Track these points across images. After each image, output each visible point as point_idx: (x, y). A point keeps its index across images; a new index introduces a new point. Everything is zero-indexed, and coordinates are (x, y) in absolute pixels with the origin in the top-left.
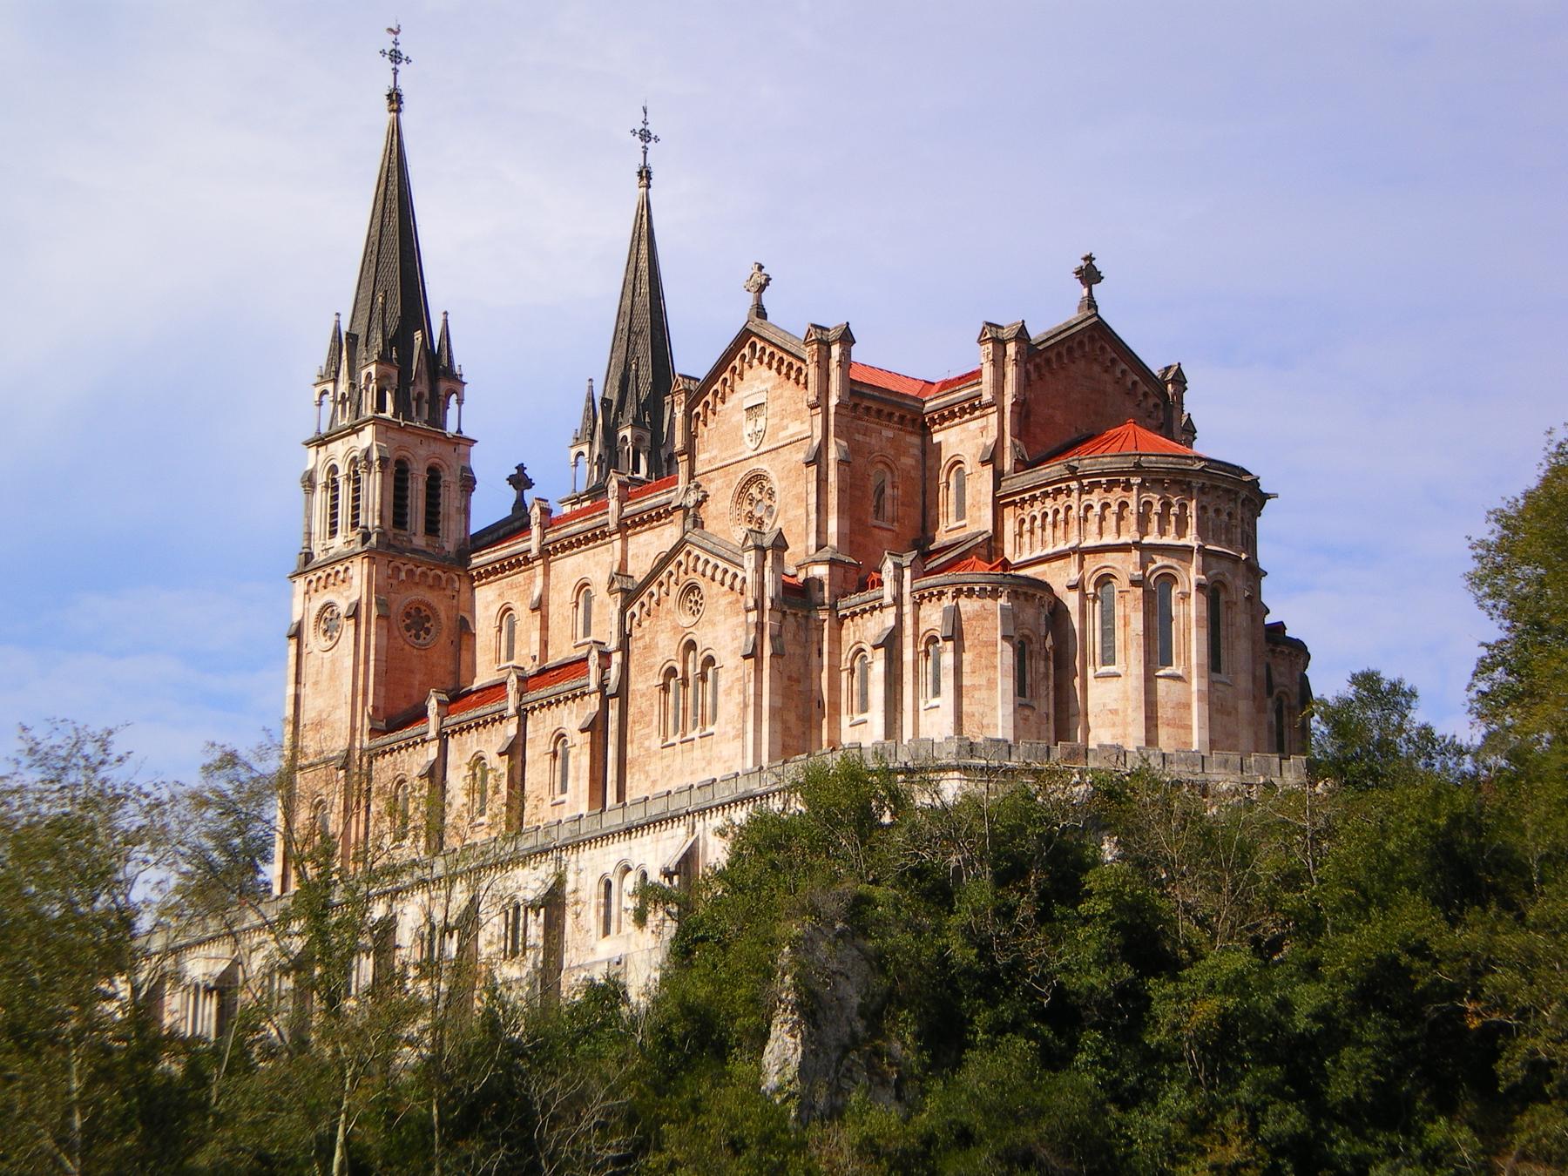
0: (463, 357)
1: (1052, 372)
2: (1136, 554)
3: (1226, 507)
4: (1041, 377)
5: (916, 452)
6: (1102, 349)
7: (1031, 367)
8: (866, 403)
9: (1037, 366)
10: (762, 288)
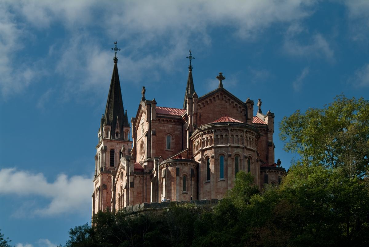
1: (208, 104)
2: (213, 150)
3: (240, 134)
4: (204, 106)
5: (180, 130)
8: (161, 119)
10: (144, 93)
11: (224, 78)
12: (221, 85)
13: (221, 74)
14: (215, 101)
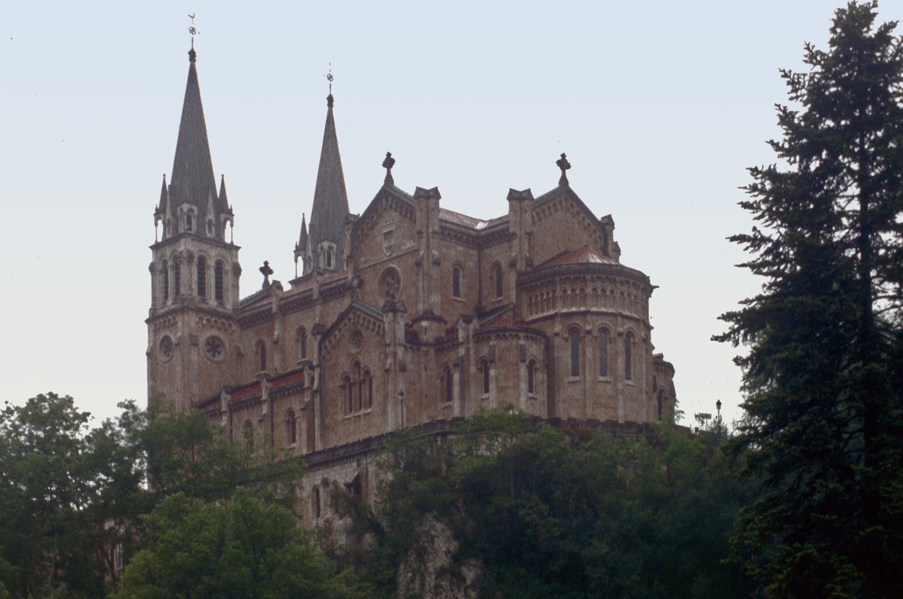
0: (231, 202)
3: (634, 292)
4: (540, 220)
5: (476, 259)
6: (572, 205)
7: (534, 214)
9: (538, 214)
11: (569, 166)
12: (564, 181)
13: (563, 156)
14: (556, 211)
